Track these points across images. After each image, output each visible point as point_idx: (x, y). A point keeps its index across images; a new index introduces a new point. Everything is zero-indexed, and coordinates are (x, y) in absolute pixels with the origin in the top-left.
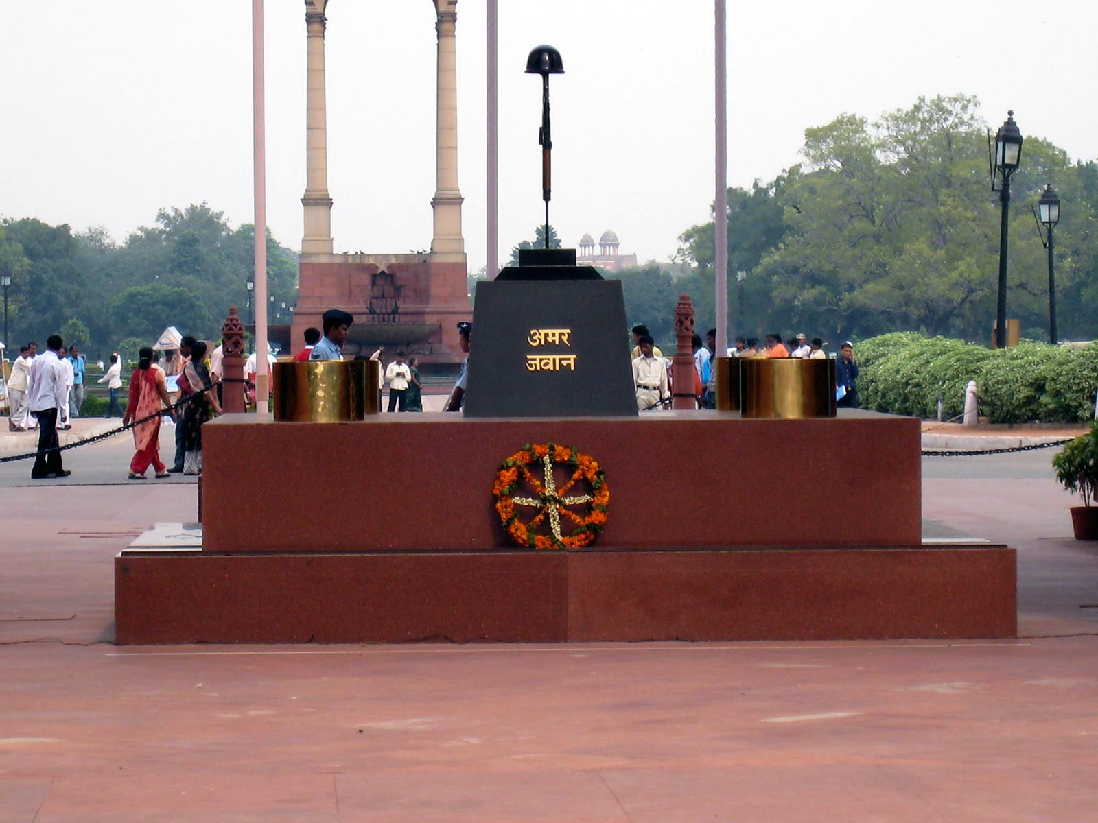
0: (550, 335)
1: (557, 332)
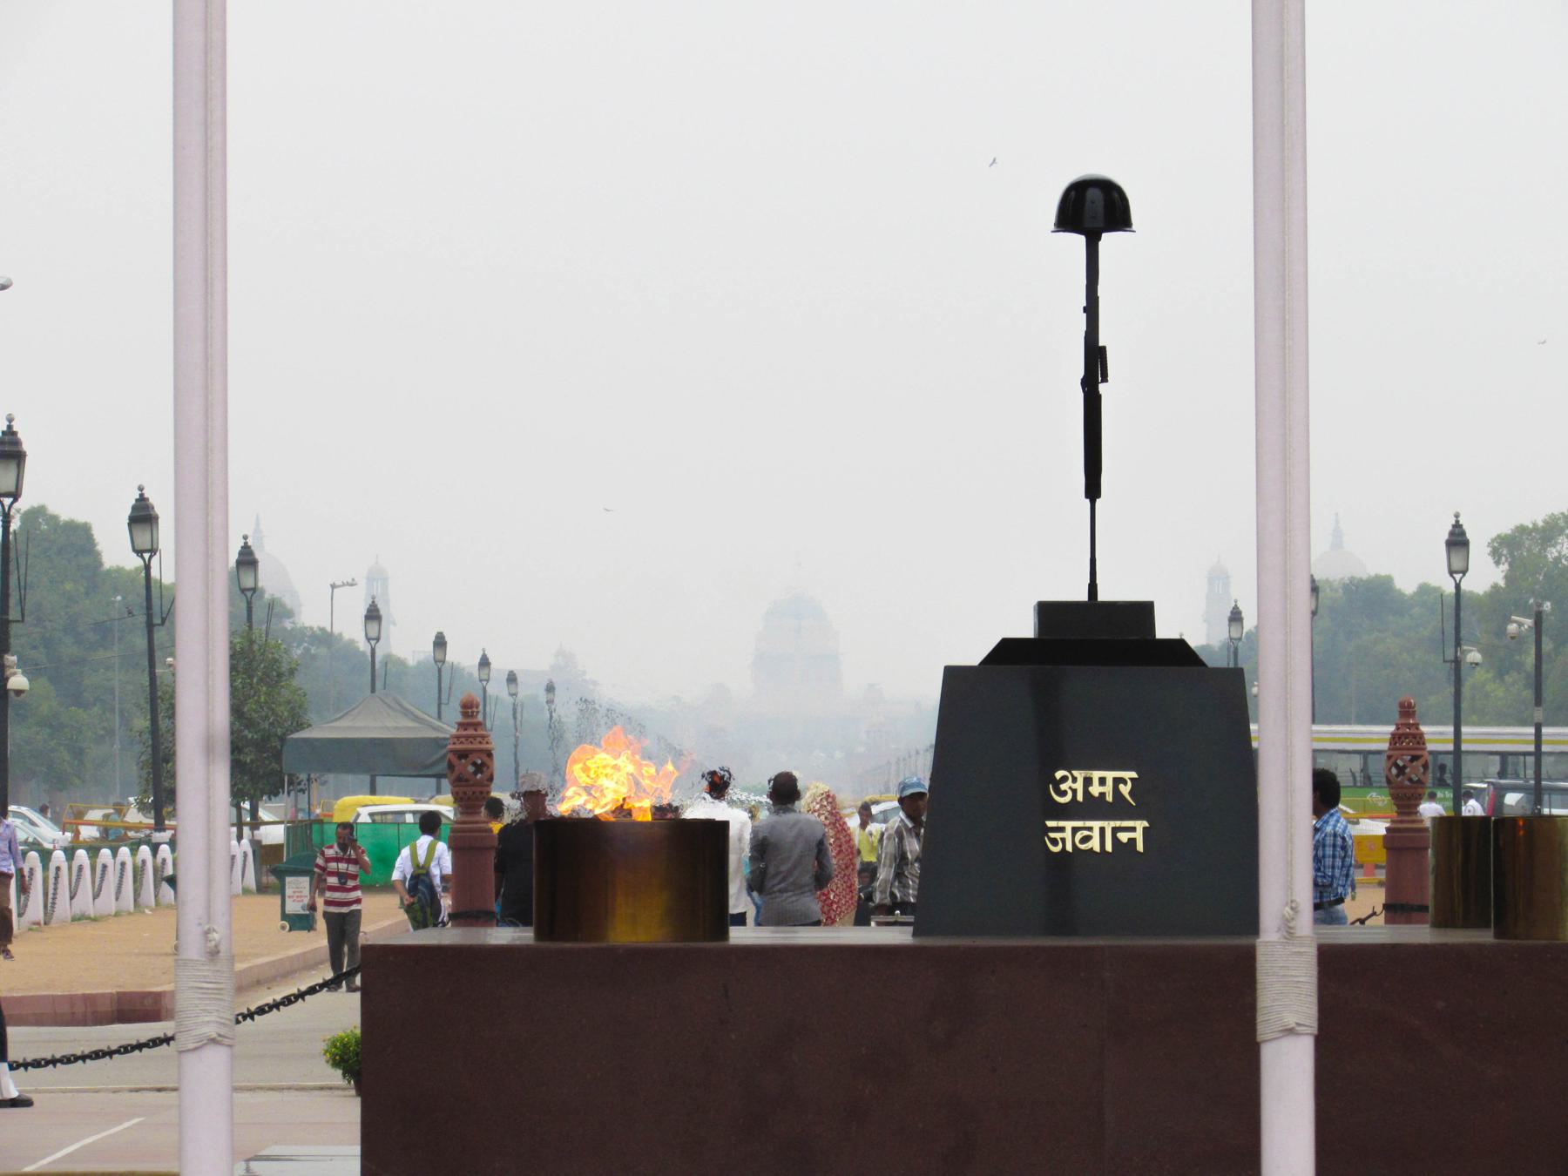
0: (1096, 781)
1: (1110, 775)
